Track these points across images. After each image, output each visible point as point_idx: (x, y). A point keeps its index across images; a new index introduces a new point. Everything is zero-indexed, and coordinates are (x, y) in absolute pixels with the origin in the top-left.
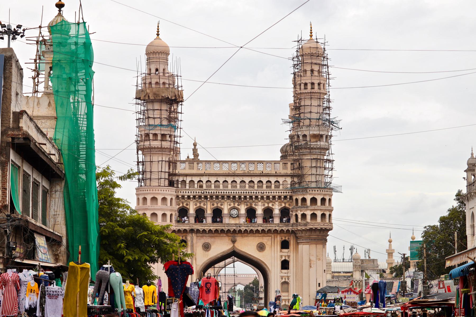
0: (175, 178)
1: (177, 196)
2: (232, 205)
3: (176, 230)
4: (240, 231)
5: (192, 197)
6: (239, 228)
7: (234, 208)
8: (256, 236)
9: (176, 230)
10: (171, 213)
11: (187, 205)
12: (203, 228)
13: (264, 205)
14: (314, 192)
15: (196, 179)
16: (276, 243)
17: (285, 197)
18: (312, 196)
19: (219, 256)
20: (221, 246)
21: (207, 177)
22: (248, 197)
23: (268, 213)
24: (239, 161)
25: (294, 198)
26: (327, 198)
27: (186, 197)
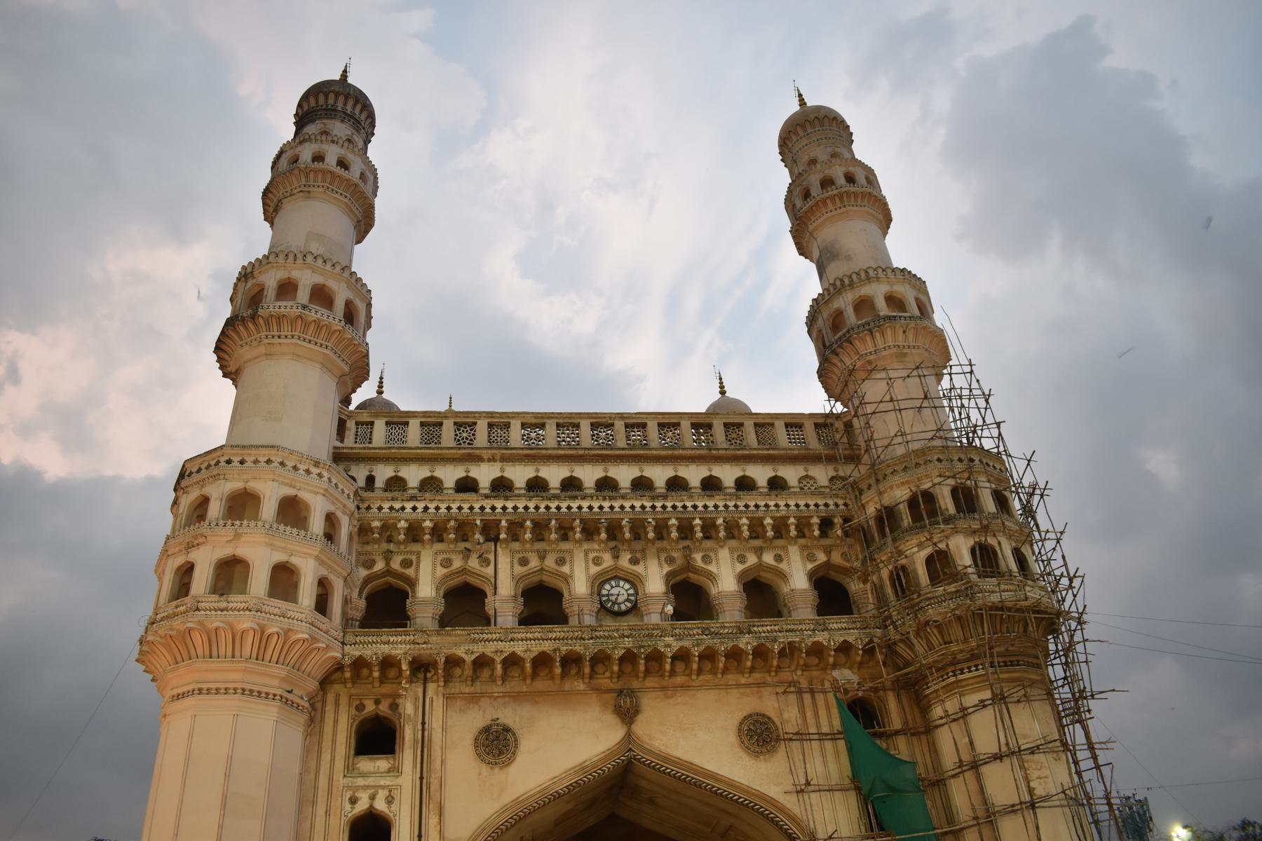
0: (361, 472)
1: (363, 531)
4: (655, 657)
5: (428, 524)
7: (614, 575)
8: (728, 686)
9: (347, 661)
10: (324, 572)
11: (407, 563)
12: (479, 649)
13: (742, 559)
15: (449, 475)
17: (826, 524)
19: (559, 787)
20: (565, 745)
21: (498, 465)
23: (761, 594)
24: (621, 416)
27: (403, 524)
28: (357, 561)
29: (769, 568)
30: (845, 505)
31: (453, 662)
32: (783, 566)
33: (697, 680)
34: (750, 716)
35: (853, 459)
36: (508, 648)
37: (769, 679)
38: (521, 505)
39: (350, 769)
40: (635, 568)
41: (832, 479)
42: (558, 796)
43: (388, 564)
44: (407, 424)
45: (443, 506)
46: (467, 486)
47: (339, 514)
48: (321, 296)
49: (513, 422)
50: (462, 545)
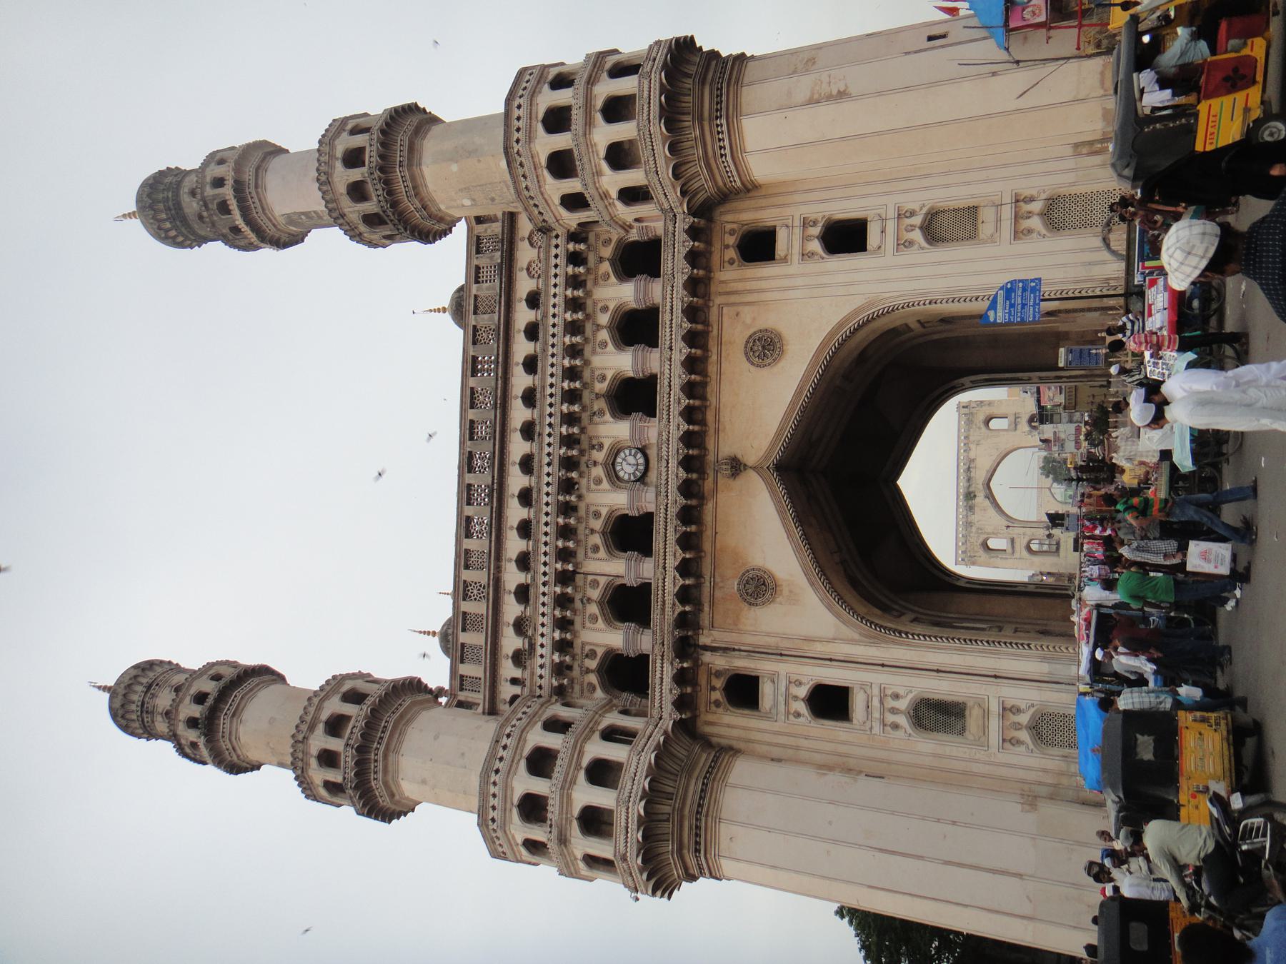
0: (507, 691)
2: (598, 471)
3: (677, 716)
4: (689, 439)
6: (674, 444)
8: (719, 373)
10: (597, 735)
11: (592, 654)
12: (669, 599)
14: (521, 124)
15: (512, 609)
16: (749, 286)
18: (540, 127)
19: (797, 534)
20: (758, 526)
22: (565, 408)
23: (637, 328)
24: (462, 443)
25: (572, 219)
26: (553, 72)
27: (556, 658)
28: (589, 698)
29: (612, 319)
30: (557, 236)
31: (683, 621)
32: (612, 306)
33: (712, 399)
34: (746, 354)
35: (511, 218)
36: (671, 572)
37: (715, 332)
38: (543, 549)
39: (767, 716)
40: (606, 445)
41: (531, 245)
42: (806, 536)
43: (592, 671)
44: (463, 645)
45: (541, 620)
46: (523, 593)
47: (544, 717)
48: (335, 726)
49: (465, 547)
50: (578, 604)
